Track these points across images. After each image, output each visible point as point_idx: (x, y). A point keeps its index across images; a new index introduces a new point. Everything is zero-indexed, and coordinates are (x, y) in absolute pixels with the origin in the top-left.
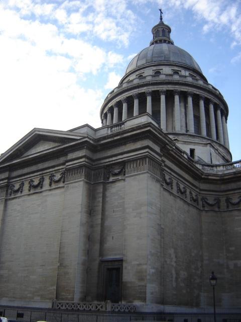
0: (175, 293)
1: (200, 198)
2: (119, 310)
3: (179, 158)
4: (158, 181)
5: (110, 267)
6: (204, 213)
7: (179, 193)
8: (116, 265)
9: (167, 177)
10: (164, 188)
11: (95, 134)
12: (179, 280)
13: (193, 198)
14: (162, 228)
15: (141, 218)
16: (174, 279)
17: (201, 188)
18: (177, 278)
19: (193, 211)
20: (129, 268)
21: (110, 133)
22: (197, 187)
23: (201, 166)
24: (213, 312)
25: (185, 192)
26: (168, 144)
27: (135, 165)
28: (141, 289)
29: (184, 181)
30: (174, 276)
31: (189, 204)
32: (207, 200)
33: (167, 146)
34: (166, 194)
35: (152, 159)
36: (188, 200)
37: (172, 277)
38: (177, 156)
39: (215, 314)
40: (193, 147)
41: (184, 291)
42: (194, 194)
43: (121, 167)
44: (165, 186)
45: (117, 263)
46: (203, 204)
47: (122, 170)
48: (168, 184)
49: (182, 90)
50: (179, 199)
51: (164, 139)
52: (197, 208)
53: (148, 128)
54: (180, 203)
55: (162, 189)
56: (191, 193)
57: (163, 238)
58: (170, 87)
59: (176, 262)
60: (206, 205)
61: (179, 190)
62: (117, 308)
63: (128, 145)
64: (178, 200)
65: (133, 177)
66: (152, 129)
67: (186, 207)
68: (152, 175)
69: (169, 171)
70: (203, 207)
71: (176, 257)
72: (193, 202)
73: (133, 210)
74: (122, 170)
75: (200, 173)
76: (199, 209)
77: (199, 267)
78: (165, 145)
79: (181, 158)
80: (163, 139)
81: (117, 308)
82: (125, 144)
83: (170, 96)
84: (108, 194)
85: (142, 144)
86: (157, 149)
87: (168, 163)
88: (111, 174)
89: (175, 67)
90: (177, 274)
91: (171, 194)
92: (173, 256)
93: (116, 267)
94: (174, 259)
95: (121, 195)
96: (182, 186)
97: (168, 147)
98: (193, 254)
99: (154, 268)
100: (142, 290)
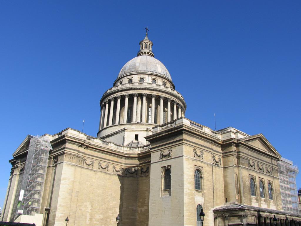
4: (73, 165)
6: (126, 178)
9: (89, 161)
14: (77, 191)
18: (91, 219)
31: (110, 174)
40: (137, 133)
44: (85, 166)
49: (139, 93)
56: (114, 167)
58: (131, 92)
64: (99, 173)
67: (107, 176)
69: (90, 157)
70: (126, 174)
71: (92, 206)
83: (131, 97)
89: (141, 75)
90: (92, 217)
96: (104, 165)
99: (62, 213)
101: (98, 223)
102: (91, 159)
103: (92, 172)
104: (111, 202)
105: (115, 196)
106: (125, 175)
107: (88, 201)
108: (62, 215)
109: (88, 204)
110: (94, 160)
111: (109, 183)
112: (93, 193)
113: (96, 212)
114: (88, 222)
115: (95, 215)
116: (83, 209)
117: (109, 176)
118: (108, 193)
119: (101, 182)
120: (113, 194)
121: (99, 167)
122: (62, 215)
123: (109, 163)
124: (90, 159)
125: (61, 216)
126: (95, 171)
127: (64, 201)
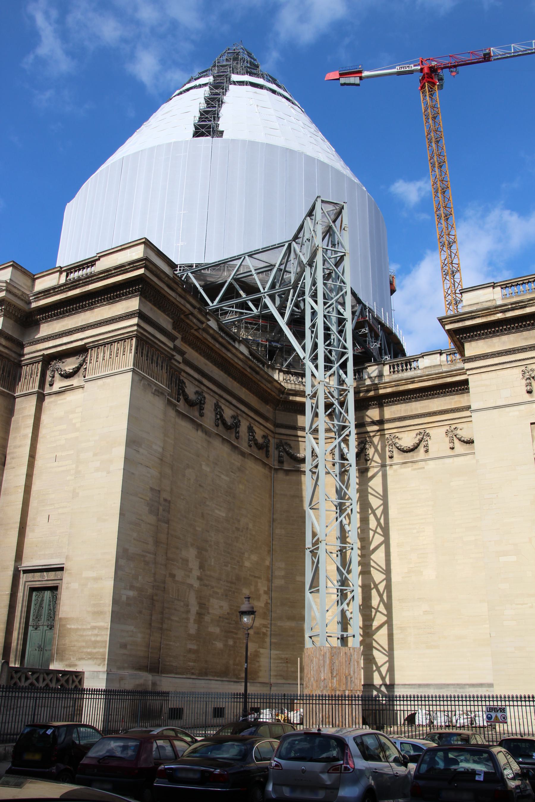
0: (195, 647)
1: (273, 442)
2: (47, 685)
3: (224, 350)
4: (159, 393)
5: (37, 584)
6: (281, 475)
7: (221, 427)
8: (47, 579)
9: (191, 390)
10: (179, 413)
11: (33, 285)
12: (207, 618)
13: (255, 440)
14: (165, 500)
15: (108, 472)
16: (192, 617)
17: (278, 421)
18: (200, 615)
19: (254, 469)
20: (75, 586)
21: (63, 280)
22: (266, 419)
23: (281, 374)
24: (243, 691)
25: (237, 425)
26: (192, 314)
27: (108, 353)
28: (97, 635)
29: (234, 402)
30: (194, 608)
31: (243, 454)
32: (291, 447)
33: (190, 316)
34: (185, 426)
35: (147, 343)
36: (244, 446)
37: (188, 612)
38: (217, 345)
39: (245, 695)
41: (219, 645)
42: (259, 433)
43: (81, 359)
44: (182, 406)
45: (52, 575)
46: (280, 456)
47: (81, 365)
48: (191, 404)
50: (221, 439)
51: (183, 301)
52: (265, 465)
53: (141, 271)
54: (221, 450)
55: (172, 413)
56: (250, 429)
57: (168, 522)
59: (199, 579)
60: (286, 458)
61: (220, 420)
62: (73, 681)
63: (96, 310)
64: (217, 443)
65: (100, 382)
66: (148, 274)
67: (236, 460)
68: (144, 378)
69: (196, 375)
70: (281, 462)
72: (255, 449)
73: (95, 455)
74: (81, 365)
75: (276, 388)
76: (270, 468)
77: (261, 592)
78: (187, 316)
79: (228, 350)
80: (179, 299)
81: (27, 678)
82: (91, 307)
84: (44, 418)
85: (128, 308)
86: (165, 322)
87: (192, 354)
88: (57, 375)
91: (199, 426)
92: (194, 564)
93: (50, 584)
94: (196, 572)
95: (74, 421)
96: (228, 413)
97: (195, 320)
98: (247, 564)
99: (132, 587)
100: (99, 638)
101: (217, 630)
102: (196, 383)
103: (200, 433)
104: (246, 555)
105: (254, 533)
106: (276, 463)
107: (192, 545)
108: (131, 593)
109: (191, 554)
110: (205, 389)
111: (241, 486)
112: (203, 515)
113: (213, 587)
114: (193, 628)
115: (212, 600)
116: (180, 574)
117: (240, 457)
118: (239, 521)
119: (223, 476)
120: (251, 526)
121: (218, 419)
122: (131, 593)
123: (239, 412)
124: (194, 382)
125: (128, 598)
126: (206, 432)
127: (135, 535)
